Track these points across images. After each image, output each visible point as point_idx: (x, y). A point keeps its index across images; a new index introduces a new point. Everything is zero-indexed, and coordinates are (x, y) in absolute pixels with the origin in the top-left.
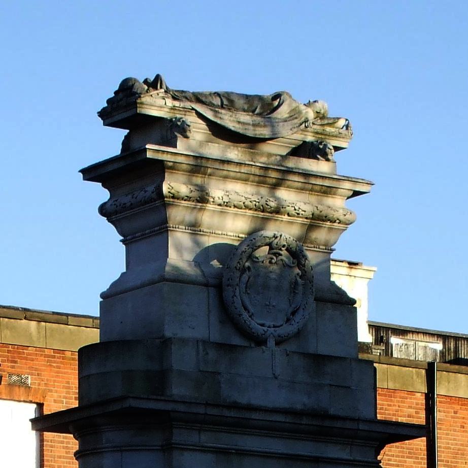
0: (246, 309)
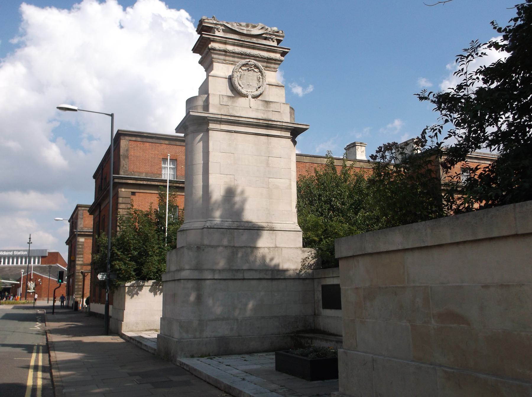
0: (240, 86)
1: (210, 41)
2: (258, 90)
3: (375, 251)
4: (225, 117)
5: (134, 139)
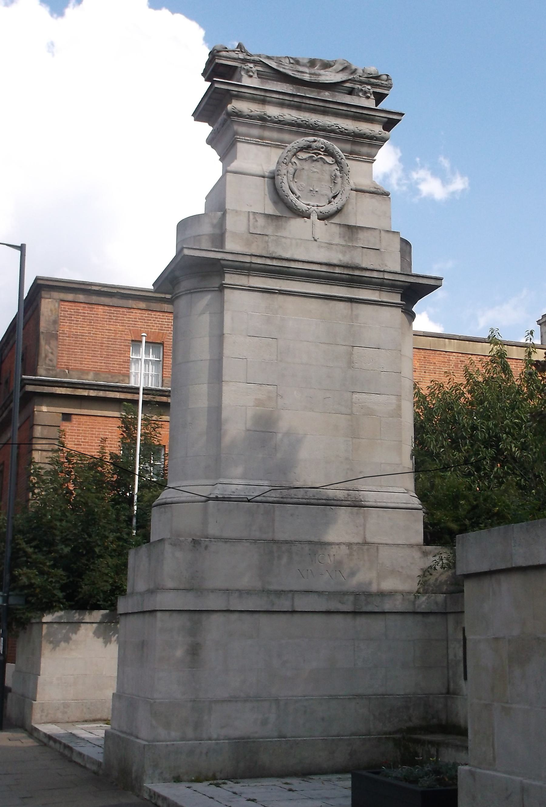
0: (293, 193)
1: (228, 96)
2: (332, 203)
3: (531, 563)
4: (259, 261)
5: (70, 297)
